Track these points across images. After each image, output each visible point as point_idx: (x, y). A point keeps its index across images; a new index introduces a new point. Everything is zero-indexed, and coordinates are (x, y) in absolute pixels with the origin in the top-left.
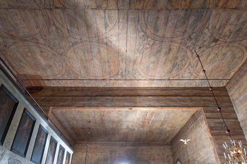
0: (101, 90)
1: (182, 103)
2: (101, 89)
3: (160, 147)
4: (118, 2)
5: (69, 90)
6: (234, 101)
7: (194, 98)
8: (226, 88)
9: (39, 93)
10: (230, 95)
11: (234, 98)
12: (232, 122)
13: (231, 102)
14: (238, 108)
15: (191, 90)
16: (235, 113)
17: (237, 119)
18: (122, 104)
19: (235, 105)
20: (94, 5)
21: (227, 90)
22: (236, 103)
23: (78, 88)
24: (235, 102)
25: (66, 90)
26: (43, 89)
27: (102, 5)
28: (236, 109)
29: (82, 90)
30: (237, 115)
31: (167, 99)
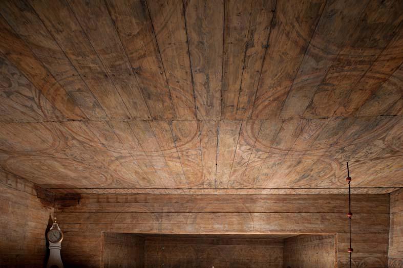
0: (175, 201)
1: (306, 225)
2: (177, 198)
3: (268, 246)
4: (197, 111)
5: (124, 200)
6: (393, 224)
7: (328, 216)
8: (391, 196)
9: (77, 206)
10: (392, 211)
11: (395, 220)
12: (377, 257)
13: (389, 224)
14: (394, 238)
15: (327, 201)
16: (388, 243)
17: (386, 252)
18: (210, 226)
19: (392, 231)
20: (146, 116)
21: (392, 200)
22: (395, 228)
23: (138, 196)
24: (394, 226)
25: (119, 200)
26: (83, 198)
27: (164, 115)
28: (392, 238)
29: (145, 200)
30: (389, 246)
31: (282, 218)
